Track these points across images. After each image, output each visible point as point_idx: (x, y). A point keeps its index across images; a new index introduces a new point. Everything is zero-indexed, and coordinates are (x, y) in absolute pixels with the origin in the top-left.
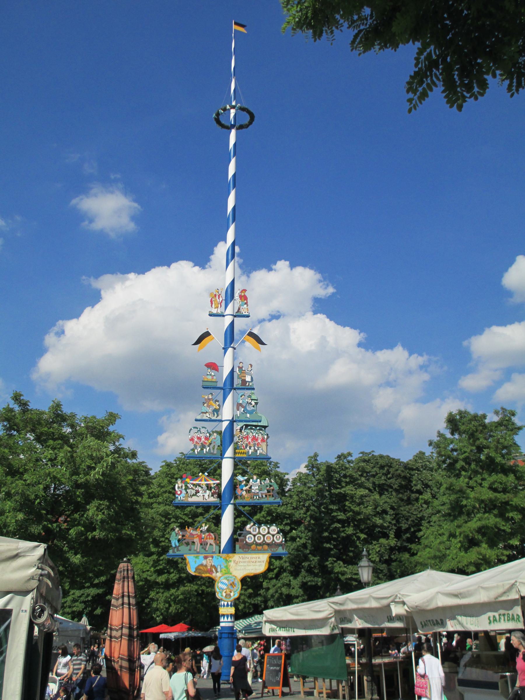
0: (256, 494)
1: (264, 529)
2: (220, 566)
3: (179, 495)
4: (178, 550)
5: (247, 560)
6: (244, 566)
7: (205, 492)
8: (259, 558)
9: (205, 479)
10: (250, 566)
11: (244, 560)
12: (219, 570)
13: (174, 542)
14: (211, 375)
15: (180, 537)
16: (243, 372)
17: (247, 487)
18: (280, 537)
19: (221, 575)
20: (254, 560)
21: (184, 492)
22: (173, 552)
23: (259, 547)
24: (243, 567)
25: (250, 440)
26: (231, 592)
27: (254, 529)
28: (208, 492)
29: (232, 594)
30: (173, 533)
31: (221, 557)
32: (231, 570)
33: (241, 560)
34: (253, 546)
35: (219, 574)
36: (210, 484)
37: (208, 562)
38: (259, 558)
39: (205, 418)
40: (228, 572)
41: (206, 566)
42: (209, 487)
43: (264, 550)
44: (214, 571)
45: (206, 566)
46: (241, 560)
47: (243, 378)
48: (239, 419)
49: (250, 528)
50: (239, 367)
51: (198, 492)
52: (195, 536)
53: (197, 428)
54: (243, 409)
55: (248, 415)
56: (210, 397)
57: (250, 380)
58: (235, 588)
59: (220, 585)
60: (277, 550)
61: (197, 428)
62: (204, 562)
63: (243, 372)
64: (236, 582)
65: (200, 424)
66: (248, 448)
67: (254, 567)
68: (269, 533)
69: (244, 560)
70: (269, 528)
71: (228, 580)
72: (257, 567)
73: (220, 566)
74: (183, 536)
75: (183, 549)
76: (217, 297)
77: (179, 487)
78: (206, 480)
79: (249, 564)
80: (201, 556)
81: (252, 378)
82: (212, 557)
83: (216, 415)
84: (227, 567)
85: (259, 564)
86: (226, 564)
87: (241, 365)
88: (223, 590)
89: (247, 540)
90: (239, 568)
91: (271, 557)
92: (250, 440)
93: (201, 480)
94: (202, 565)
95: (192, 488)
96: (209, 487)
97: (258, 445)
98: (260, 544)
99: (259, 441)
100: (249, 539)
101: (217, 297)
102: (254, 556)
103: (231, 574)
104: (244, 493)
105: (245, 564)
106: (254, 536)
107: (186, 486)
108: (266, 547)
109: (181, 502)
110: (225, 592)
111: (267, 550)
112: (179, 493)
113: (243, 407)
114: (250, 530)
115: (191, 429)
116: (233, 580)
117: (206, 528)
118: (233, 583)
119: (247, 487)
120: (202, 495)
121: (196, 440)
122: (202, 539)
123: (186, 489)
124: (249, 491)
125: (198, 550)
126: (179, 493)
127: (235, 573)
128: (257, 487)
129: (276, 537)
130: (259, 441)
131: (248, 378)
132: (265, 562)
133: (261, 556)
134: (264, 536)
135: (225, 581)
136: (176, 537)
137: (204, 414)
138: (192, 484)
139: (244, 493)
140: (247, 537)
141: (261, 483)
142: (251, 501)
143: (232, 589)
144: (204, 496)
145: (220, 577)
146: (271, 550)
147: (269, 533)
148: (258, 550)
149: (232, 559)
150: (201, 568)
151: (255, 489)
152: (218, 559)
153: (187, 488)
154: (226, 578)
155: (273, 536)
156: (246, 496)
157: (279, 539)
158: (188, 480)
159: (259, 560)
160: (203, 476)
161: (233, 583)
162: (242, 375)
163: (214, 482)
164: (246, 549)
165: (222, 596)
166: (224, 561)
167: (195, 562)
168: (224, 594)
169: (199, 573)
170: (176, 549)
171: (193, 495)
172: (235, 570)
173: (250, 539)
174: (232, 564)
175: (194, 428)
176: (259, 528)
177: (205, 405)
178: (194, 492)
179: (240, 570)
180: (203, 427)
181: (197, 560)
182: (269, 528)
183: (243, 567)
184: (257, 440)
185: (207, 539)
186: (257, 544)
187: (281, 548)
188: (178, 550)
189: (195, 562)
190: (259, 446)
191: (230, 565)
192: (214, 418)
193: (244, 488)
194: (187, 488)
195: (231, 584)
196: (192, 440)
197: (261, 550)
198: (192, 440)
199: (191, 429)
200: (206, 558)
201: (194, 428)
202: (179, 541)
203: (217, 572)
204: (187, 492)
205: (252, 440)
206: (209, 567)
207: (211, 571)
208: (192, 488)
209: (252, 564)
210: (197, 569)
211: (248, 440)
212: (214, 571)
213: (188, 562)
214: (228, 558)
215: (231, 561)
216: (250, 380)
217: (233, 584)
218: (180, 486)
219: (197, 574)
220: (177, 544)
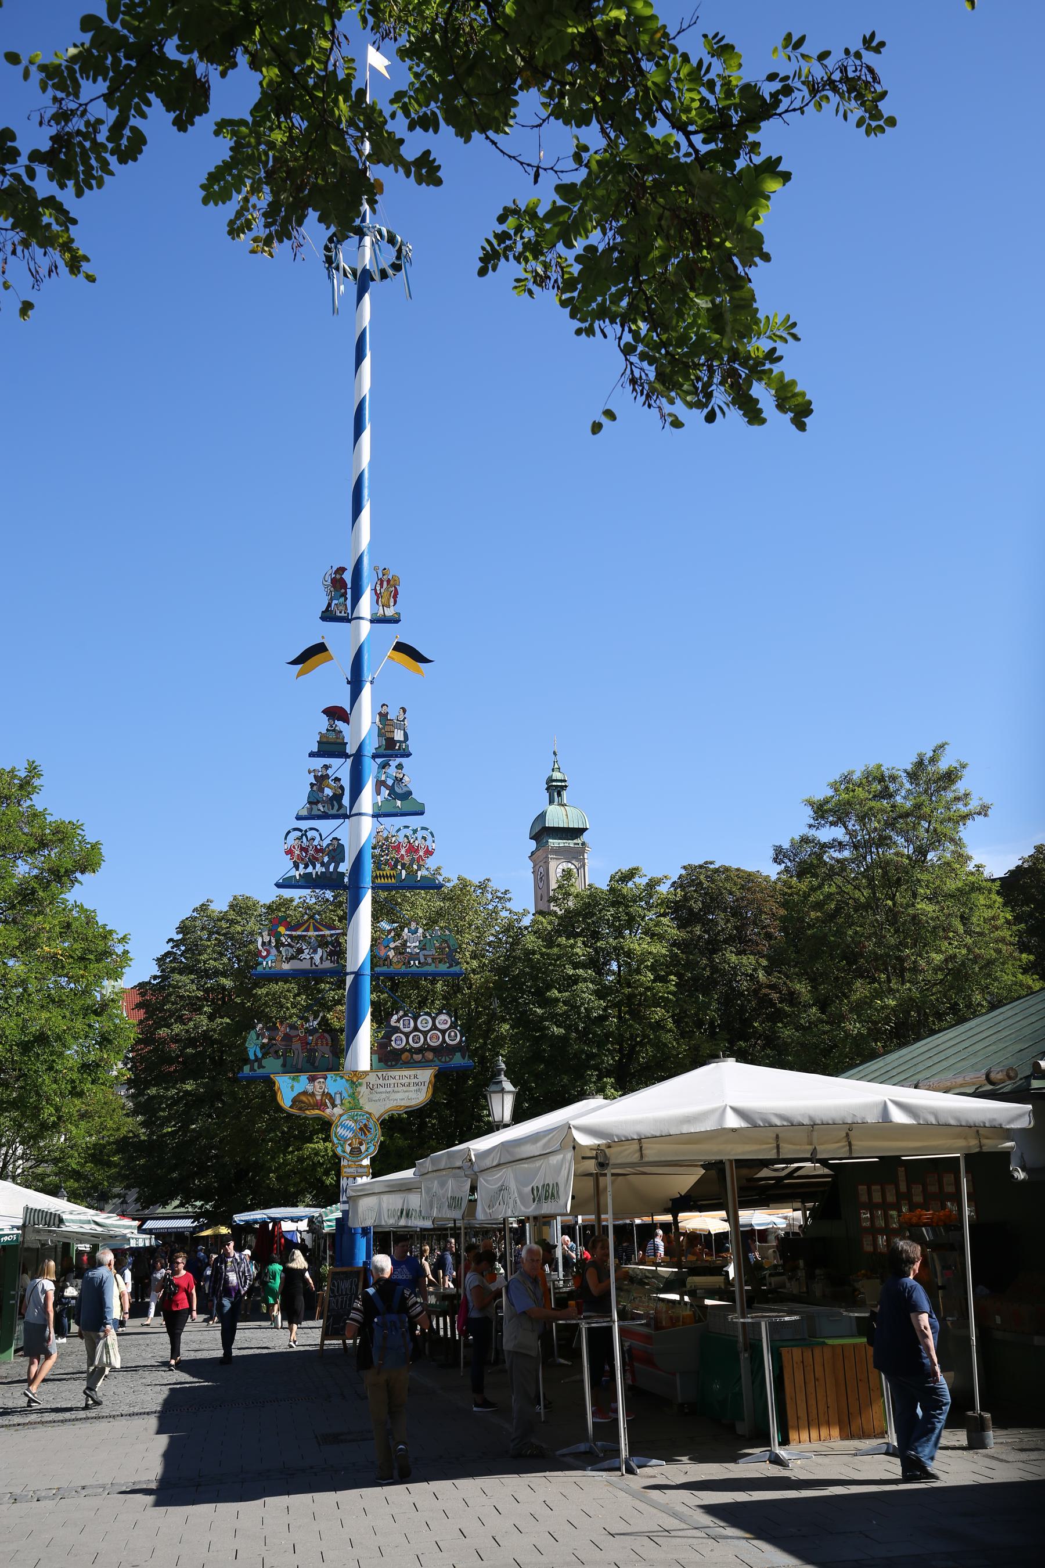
0: (414, 956)
1: (424, 1022)
2: (341, 1094)
3: (264, 958)
4: (261, 1066)
5: (392, 1081)
6: (387, 1092)
7: (315, 952)
8: (415, 1077)
9: (314, 926)
12: (338, 1102)
13: (253, 1049)
15: (265, 1041)
16: (388, 722)
17: (397, 943)
18: (456, 1035)
19: (341, 1112)
20: (405, 1081)
21: (274, 951)
22: (252, 1069)
23: (418, 1057)
24: (384, 1096)
25: (403, 852)
26: (361, 1144)
28: (320, 951)
29: (363, 1148)
30: (253, 1034)
31: (342, 1077)
32: (361, 1101)
33: (381, 1082)
34: (405, 1056)
35: (338, 1111)
36: (323, 936)
37: (317, 1088)
38: (415, 1077)
39: (315, 812)
40: (355, 1106)
41: (313, 1095)
42: (322, 942)
43: (427, 1061)
44: (329, 1104)
45: (313, 1095)
46: (381, 1082)
47: (389, 735)
48: (383, 811)
50: (380, 714)
51: (300, 951)
52: (294, 1040)
53: (300, 830)
54: (388, 792)
55: (399, 803)
57: (402, 739)
58: (369, 1136)
59: (341, 1131)
60: (451, 1059)
61: (300, 830)
62: (310, 1088)
63: (388, 722)
64: (371, 1125)
65: (304, 825)
66: (399, 867)
68: (434, 1027)
70: (434, 1019)
71: (356, 1121)
72: (412, 1095)
73: (341, 1094)
74: (270, 1039)
75: (271, 1064)
77: (264, 944)
78: (316, 929)
79: (396, 1089)
80: (304, 1078)
81: (406, 735)
82: (325, 1078)
83: (336, 806)
84: (353, 1096)
85: (415, 1088)
86: (350, 1091)
87: (384, 710)
88: (346, 1140)
89: (393, 1043)
90: (376, 1097)
91: (436, 1076)
92: (403, 852)
93: (307, 930)
94: (305, 1093)
95: (289, 945)
96: (322, 942)
97: (418, 862)
98: (420, 1051)
99: (421, 853)
100: (398, 1042)
102: (407, 1073)
103: (361, 1108)
104: (391, 954)
105: (388, 1089)
106: (407, 1035)
107: (278, 941)
108: (430, 1055)
109: (267, 969)
110: (350, 1145)
111: (432, 1061)
112: (264, 954)
113: (387, 787)
115: (289, 832)
116: (364, 1122)
117: (315, 1023)
118: (365, 1125)
119: (397, 943)
120: (308, 957)
121: (297, 852)
122: (308, 1044)
123: (277, 947)
124: (400, 951)
125: (299, 1067)
126: (264, 954)
127: (368, 1107)
130: (421, 853)
131: (398, 736)
133: (419, 1072)
134: (425, 1034)
135: (351, 1123)
136: (259, 1042)
137: (314, 806)
138: (290, 936)
139: (391, 954)
141: (425, 937)
142: (403, 968)
143: (363, 1137)
144: (312, 958)
145: (341, 1116)
146: (440, 1060)
147: (434, 1027)
148: (416, 1062)
149: (364, 1081)
150: (304, 1099)
151: (413, 946)
152: (335, 1081)
153: (279, 944)
154: (352, 1118)
155: (443, 1032)
156: (395, 960)
157: (455, 1038)
158: (282, 929)
159: (416, 1080)
160: (311, 921)
161: (365, 1125)
162: (387, 728)
163: (333, 932)
164: (391, 1061)
165: (344, 1152)
166: (348, 1085)
167: (292, 1088)
168: (348, 1149)
169: (300, 1109)
170: (256, 1064)
171: (293, 958)
172: (370, 1100)
173: (399, 1042)
174: (363, 1090)
175: (295, 829)
176: (415, 1019)
178: (292, 951)
180: (311, 829)
181: (296, 1084)
182: (434, 1019)
183: (384, 1096)
184: (417, 851)
185: (317, 1044)
186: (412, 1051)
187: (458, 1055)
188: (261, 1066)
189: (292, 1088)
190: (421, 863)
191: (359, 1093)
192: (334, 812)
193: (392, 945)
194: (279, 944)
195: (361, 1129)
196: (289, 852)
197: (419, 1062)
198: (289, 852)
199: (289, 832)
200: (312, 1079)
201: (295, 829)
202: (263, 1046)
203: (334, 1106)
204: (280, 952)
205: (407, 851)
206: (319, 1098)
207: (321, 1105)
208: (289, 945)
209: (401, 1088)
210: (295, 1101)
211: (398, 851)
212: (329, 1104)
213: (279, 1088)
215: (360, 1084)
216: (402, 739)
217: (364, 1129)
218: (267, 939)
219: (294, 1111)
220: (260, 1055)
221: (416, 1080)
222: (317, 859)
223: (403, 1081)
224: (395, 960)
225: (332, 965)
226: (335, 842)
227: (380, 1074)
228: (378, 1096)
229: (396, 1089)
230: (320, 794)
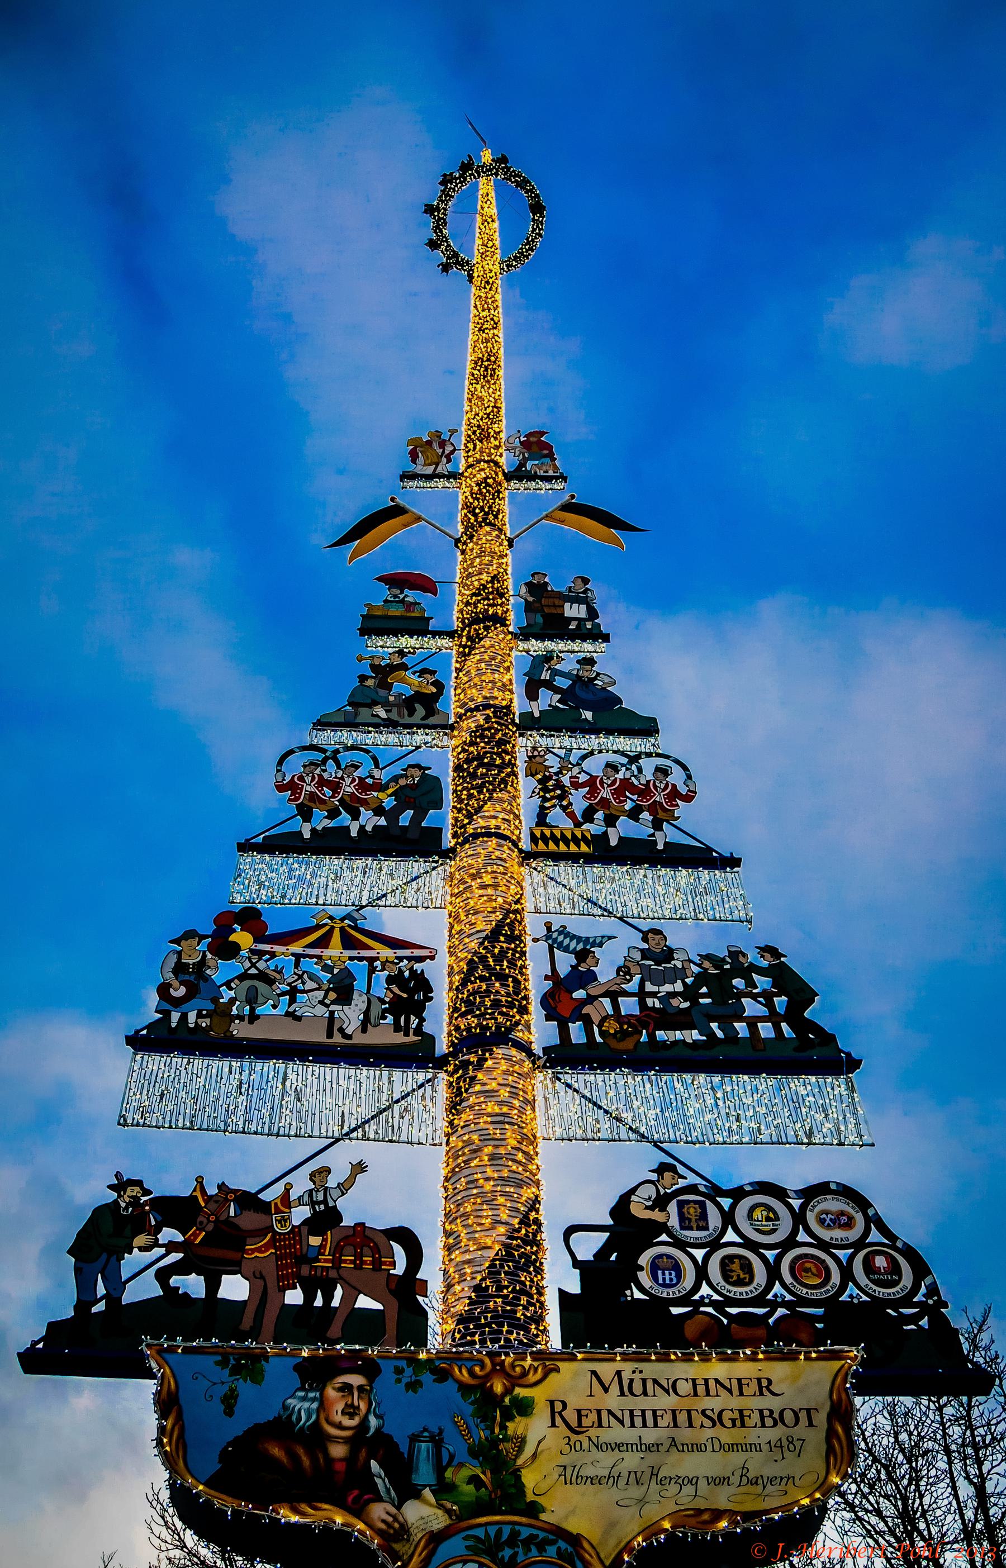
5: (665, 1402)
7: (345, 996)
10: (698, 1448)
11: (640, 1403)
14: (403, 601)
24: (631, 1460)
27: (692, 1211)
46: (613, 1400)
49: (661, 1202)
56: (397, 661)
67: (737, 1458)
69: (640, 1403)
76: (435, 446)
85: (772, 1434)
89: (644, 1277)
93: (323, 942)
101: (435, 446)
114: (657, 1216)
128: (679, 987)
129: (868, 1266)
132: (821, 1418)
140: (644, 1259)
149: (539, 1395)
152: (413, 1386)
159: (767, 1402)
177: (370, 682)
179: (613, 1478)
183: (631, 1460)
191: (521, 1442)
214: (498, 1388)
215: (524, 1408)
221: (767, 1402)
222: (365, 803)
223: (714, 1404)
224: (612, 1027)
225: (400, 1038)
226: (418, 773)
227: (606, 1370)
228: (607, 1459)
229: (685, 1435)
230: (382, 692)
